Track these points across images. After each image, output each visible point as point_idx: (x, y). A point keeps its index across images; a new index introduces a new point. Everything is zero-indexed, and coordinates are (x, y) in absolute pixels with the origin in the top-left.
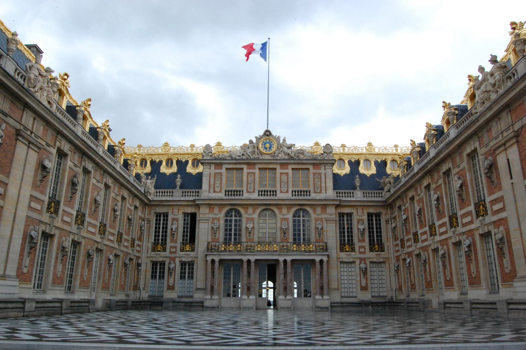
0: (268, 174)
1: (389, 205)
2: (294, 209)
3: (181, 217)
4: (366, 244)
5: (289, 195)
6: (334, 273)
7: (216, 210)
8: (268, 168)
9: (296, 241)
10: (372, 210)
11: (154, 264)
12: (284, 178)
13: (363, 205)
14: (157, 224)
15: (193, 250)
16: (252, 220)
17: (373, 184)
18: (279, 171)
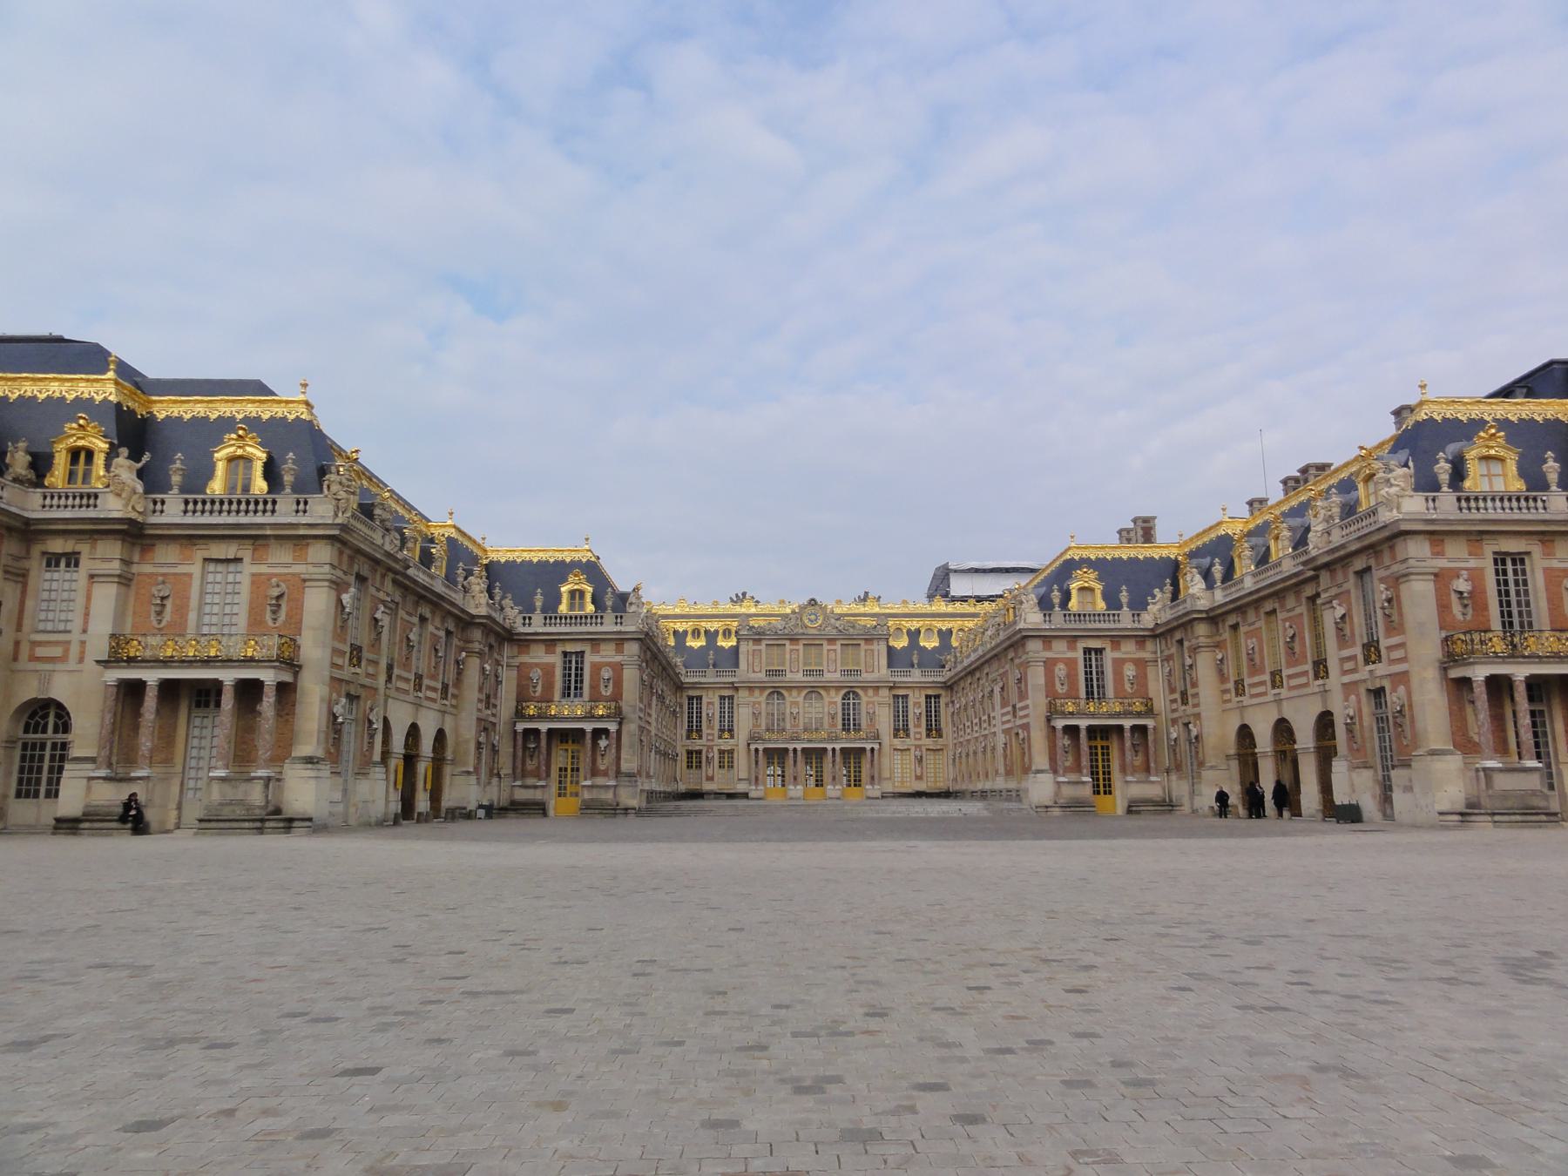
0: (813, 650)
1: (949, 687)
2: (843, 692)
3: (717, 701)
4: (923, 730)
5: (837, 676)
6: (886, 761)
7: (757, 693)
8: (813, 643)
9: (846, 728)
10: (930, 692)
11: (690, 753)
12: (832, 655)
13: (921, 687)
14: (690, 708)
15: (732, 737)
16: (796, 703)
17: (931, 661)
18: (826, 647)
